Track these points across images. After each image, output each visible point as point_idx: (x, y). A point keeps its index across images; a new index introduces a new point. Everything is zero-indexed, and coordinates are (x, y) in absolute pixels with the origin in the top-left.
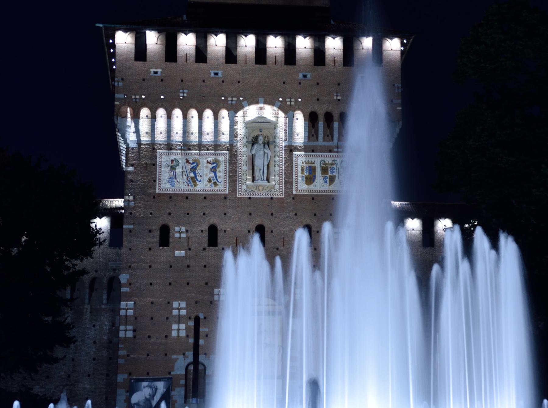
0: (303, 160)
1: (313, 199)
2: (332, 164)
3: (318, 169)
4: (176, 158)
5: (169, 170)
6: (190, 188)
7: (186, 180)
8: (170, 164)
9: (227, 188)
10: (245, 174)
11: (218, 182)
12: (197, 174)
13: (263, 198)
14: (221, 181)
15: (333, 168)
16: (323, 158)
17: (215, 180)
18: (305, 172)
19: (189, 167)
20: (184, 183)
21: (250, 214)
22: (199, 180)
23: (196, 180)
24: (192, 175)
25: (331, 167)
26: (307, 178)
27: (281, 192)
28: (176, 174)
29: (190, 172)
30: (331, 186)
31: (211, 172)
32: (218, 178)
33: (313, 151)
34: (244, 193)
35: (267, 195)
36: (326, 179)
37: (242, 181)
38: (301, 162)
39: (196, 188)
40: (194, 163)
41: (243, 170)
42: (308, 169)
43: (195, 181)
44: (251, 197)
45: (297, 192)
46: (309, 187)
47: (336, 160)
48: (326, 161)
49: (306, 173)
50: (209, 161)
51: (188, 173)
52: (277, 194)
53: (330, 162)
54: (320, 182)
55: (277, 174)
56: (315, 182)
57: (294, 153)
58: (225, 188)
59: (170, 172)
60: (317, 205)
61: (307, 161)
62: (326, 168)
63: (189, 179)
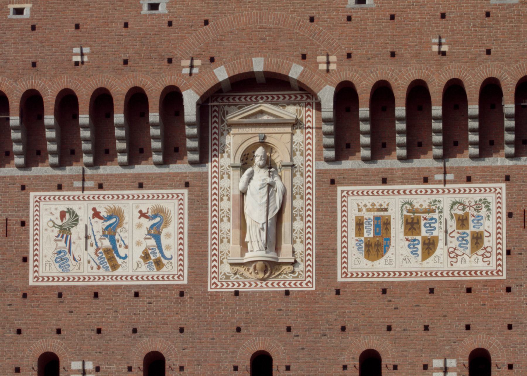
0: (360, 204)
1: (384, 291)
2: (430, 211)
3: (397, 221)
4: (70, 207)
5: (57, 235)
6: (102, 272)
7: (94, 256)
8: (59, 222)
9: (186, 271)
10: (225, 240)
11: (166, 258)
12: (118, 241)
13: (268, 292)
14: (171, 255)
15: (432, 219)
16: (408, 198)
17: (159, 255)
18: (365, 230)
19: (99, 226)
20: (89, 262)
21: (239, 330)
22: (124, 256)
23: (115, 255)
24: (107, 243)
25: (427, 217)
26: (368, 245)
27: (307, 280)
28: (72, 241)
29: (103, 237)
30: (427, 261)
31: (148, 236)
32: (164, 249)
33: (384, 181)
34: (224, 283)
35: (275, 284)
36: (414, 245)
37: (220, 255)
38: (356, 208)
39: (116, 273)
40: (109, 218)
41: (221, 231)
42: (372, 223)
43: (114, 257)
44: (240, 290)
45: (346, 277)
46: (375, 267)
47: (439, 201)
48: (414, 203)
49: (369, 233)
50: (144, 211)
51: (97, 240)
52: (299, 282)
53: (426, 206)
54: (401, 252)
55: (300, 238)
56: (388, 254)
57: (339, 189)
58: (181, 272)
59: (57, 239)
60: (394, 306)
61: (369, 206)
62: (415, 221)
63: (101, 253)
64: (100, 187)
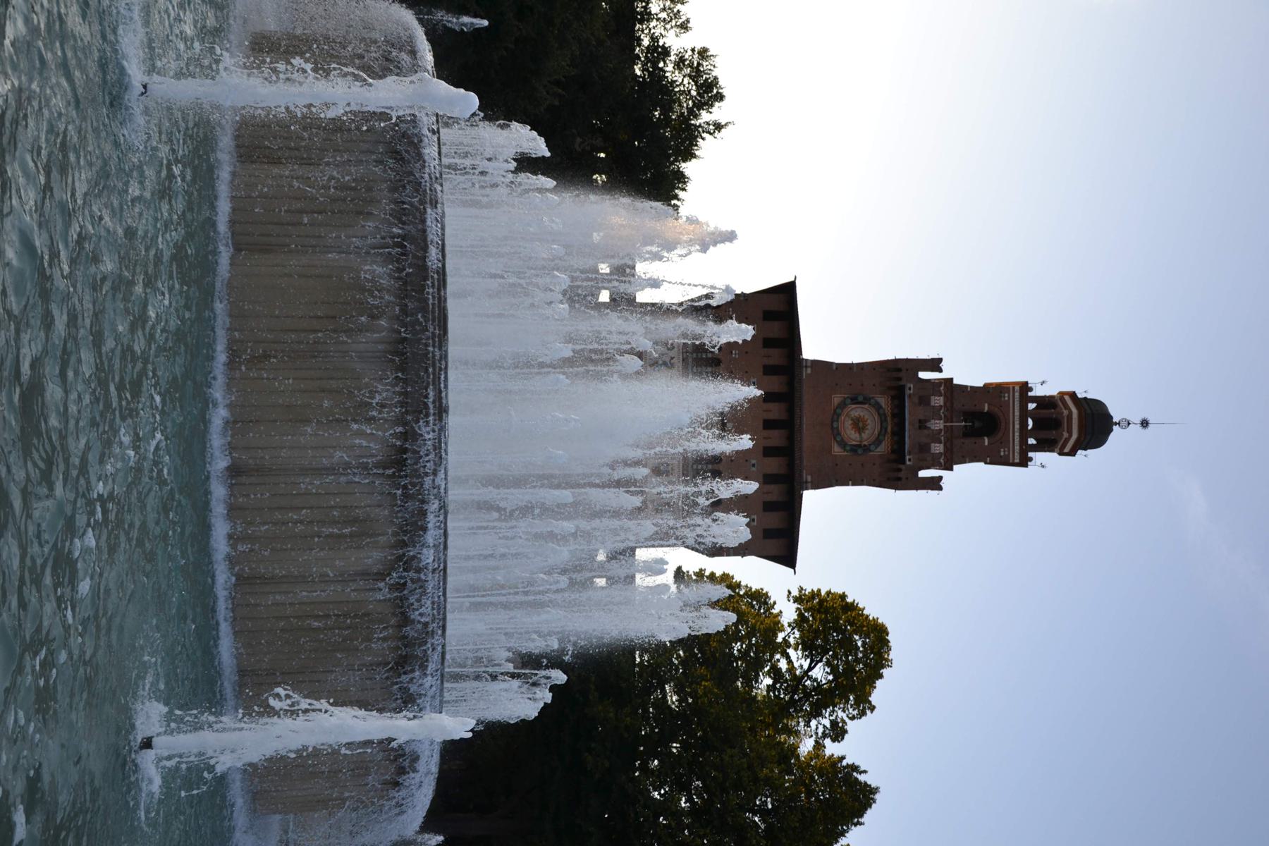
19: (667, 360)
64: (683, 360)
